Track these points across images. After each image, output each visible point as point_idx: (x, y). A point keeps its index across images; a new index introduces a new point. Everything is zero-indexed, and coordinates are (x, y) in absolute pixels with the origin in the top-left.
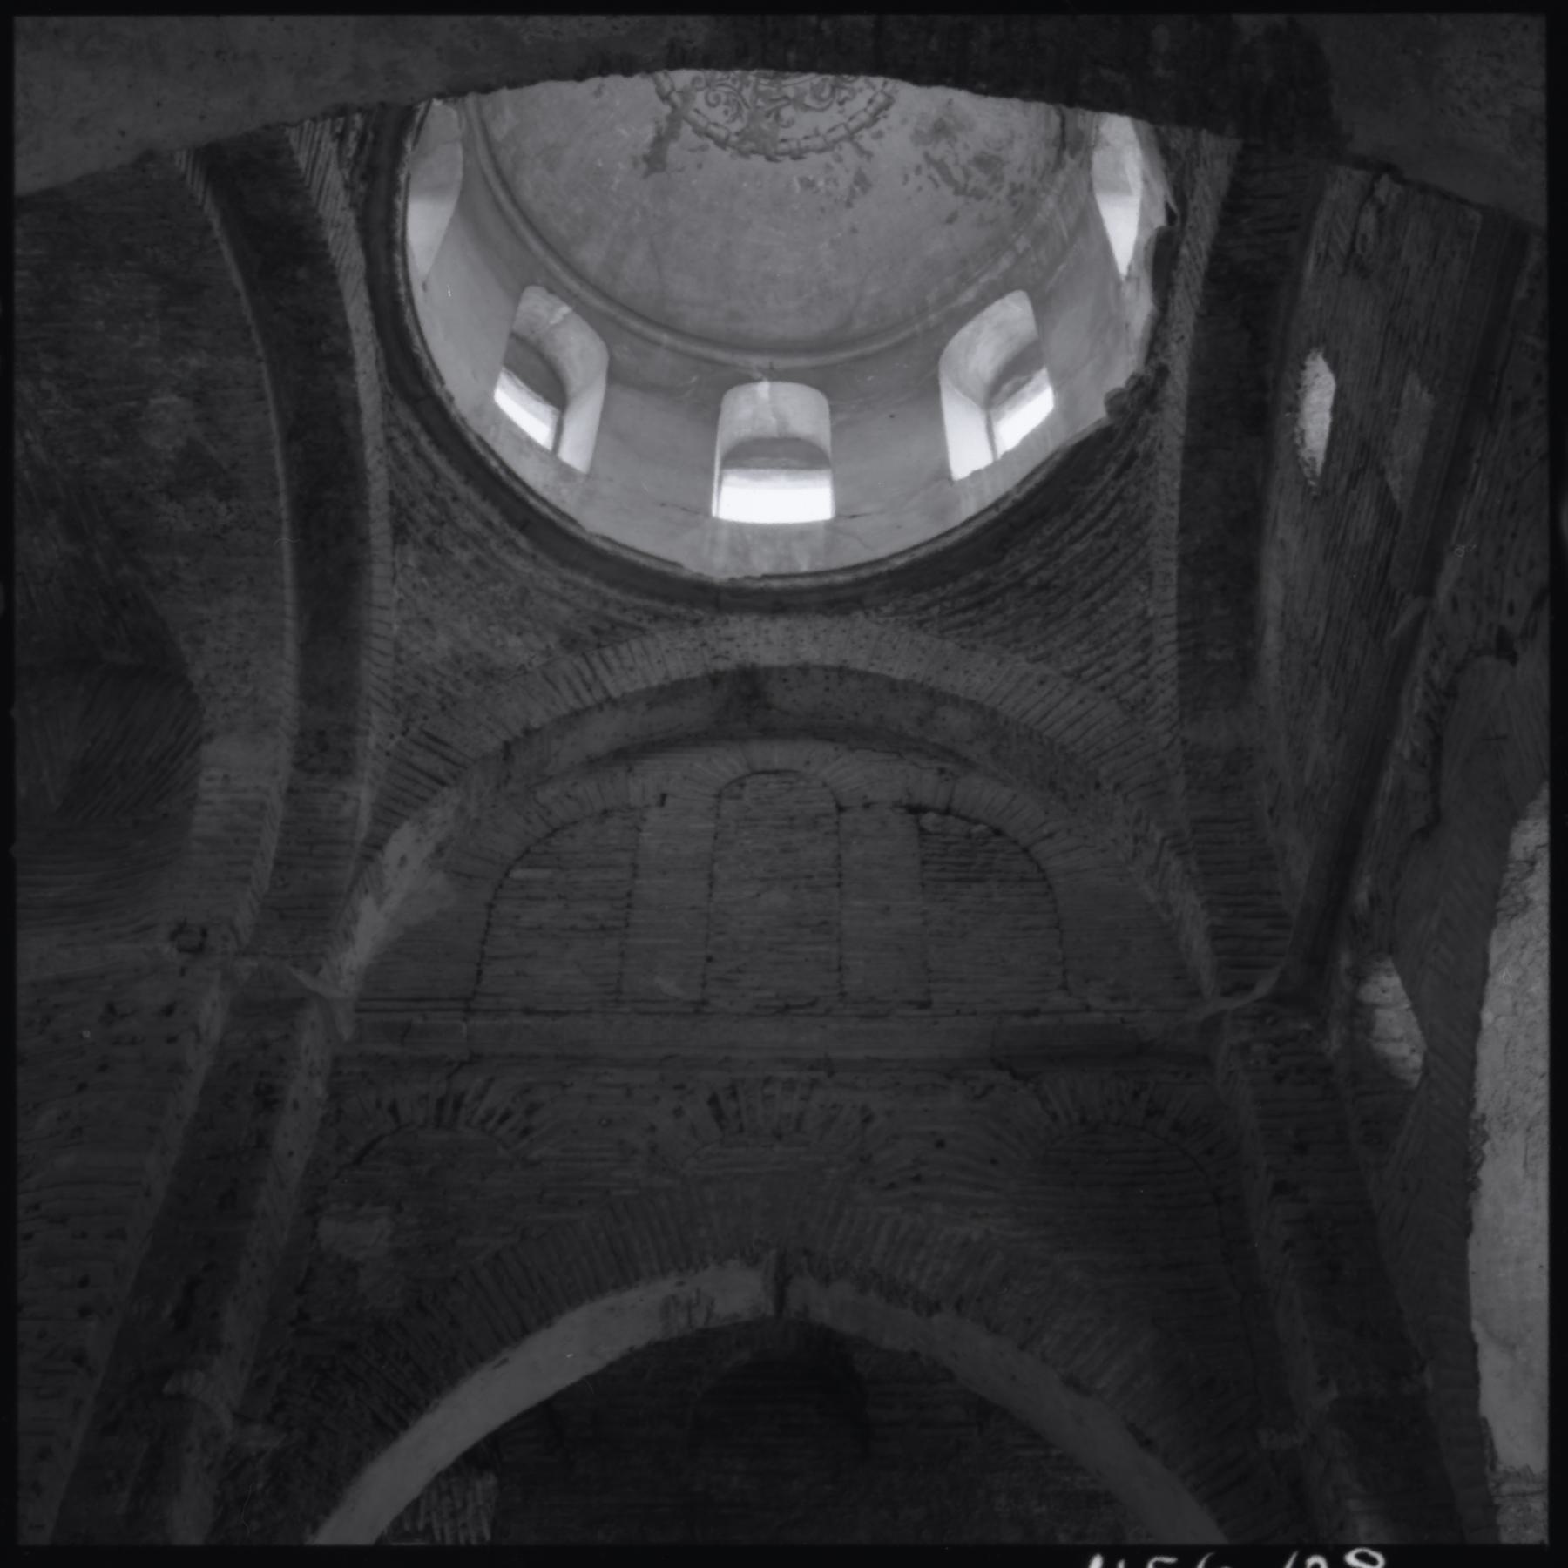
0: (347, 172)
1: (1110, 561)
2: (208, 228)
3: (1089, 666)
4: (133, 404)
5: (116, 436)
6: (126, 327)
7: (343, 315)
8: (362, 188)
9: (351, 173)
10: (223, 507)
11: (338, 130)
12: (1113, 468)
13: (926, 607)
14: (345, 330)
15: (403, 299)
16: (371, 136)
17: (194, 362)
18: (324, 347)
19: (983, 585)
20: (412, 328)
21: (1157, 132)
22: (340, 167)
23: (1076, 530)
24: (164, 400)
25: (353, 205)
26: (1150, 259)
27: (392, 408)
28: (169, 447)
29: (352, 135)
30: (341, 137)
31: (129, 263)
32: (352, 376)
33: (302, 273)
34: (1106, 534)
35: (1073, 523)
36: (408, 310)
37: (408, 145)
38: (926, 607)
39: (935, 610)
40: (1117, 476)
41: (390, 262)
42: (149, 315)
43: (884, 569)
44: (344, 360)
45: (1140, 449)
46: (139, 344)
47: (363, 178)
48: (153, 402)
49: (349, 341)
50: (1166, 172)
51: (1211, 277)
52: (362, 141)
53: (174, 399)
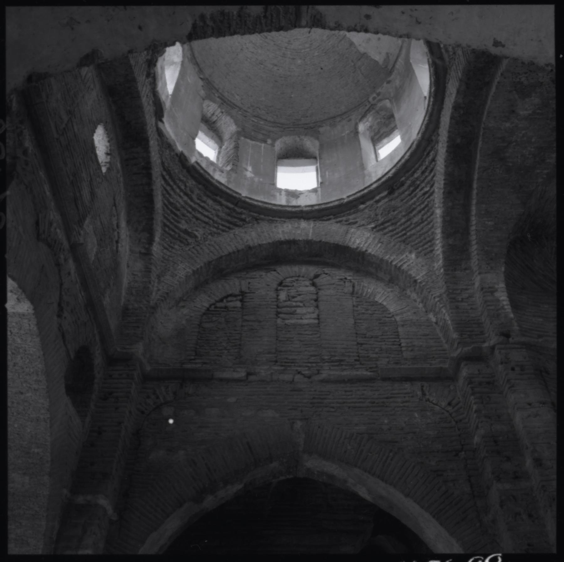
0: (436, 146)
2: (478, 179)
4: (538, 111)
5: (551, 102)
6: (525, 139)
7: (450, 123)
8: (434, 138)
9: (435, 145)
10: (523, 79)
11: (433, 163)
14: (452, 118)
15: (432, 95)
16: (425, 154)
17: (508, 125)
18: (462, 112)
20: (433, 85)
21: (173, 150)
22: (437, 150)
24: (525, 112)
25: (438, 135)
26: (163, 105)
27: (450, 62)
28: (533, 98)
29: (431, 158)
30: (434, 160)
31: (511, 164)
32: (455, 102)
33: (459, 141)
36: (433, 90)
37: (414, 146)
41: (433, 109)
42: (514, 144)
44: (456, 107)
46: (523, 132)
47: (432, 141)
48: (530, 112)
49: (452, 113)
50: (167, 139)
51: (147, 140)
52: (428, 154)
53: (521, 113)
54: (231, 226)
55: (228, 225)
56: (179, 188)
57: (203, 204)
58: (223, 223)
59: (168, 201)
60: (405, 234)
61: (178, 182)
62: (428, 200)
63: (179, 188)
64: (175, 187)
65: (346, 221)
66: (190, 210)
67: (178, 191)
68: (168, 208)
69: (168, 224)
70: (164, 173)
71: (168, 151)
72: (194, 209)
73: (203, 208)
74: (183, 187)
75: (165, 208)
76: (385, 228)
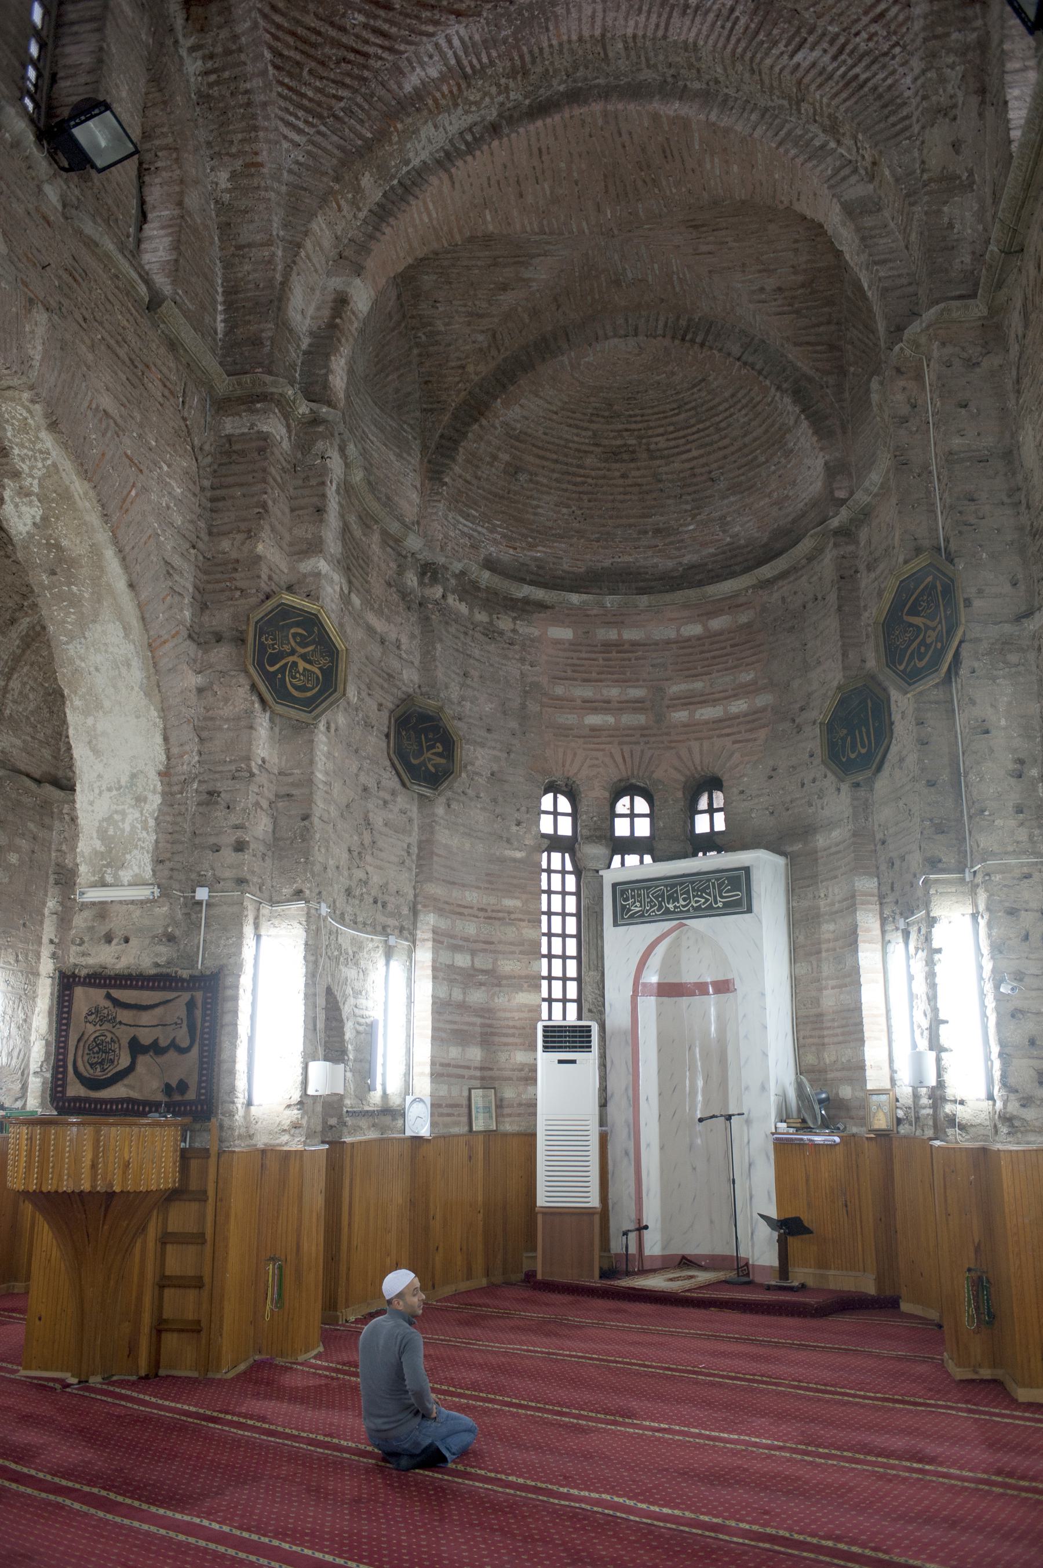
62: (380, 51)
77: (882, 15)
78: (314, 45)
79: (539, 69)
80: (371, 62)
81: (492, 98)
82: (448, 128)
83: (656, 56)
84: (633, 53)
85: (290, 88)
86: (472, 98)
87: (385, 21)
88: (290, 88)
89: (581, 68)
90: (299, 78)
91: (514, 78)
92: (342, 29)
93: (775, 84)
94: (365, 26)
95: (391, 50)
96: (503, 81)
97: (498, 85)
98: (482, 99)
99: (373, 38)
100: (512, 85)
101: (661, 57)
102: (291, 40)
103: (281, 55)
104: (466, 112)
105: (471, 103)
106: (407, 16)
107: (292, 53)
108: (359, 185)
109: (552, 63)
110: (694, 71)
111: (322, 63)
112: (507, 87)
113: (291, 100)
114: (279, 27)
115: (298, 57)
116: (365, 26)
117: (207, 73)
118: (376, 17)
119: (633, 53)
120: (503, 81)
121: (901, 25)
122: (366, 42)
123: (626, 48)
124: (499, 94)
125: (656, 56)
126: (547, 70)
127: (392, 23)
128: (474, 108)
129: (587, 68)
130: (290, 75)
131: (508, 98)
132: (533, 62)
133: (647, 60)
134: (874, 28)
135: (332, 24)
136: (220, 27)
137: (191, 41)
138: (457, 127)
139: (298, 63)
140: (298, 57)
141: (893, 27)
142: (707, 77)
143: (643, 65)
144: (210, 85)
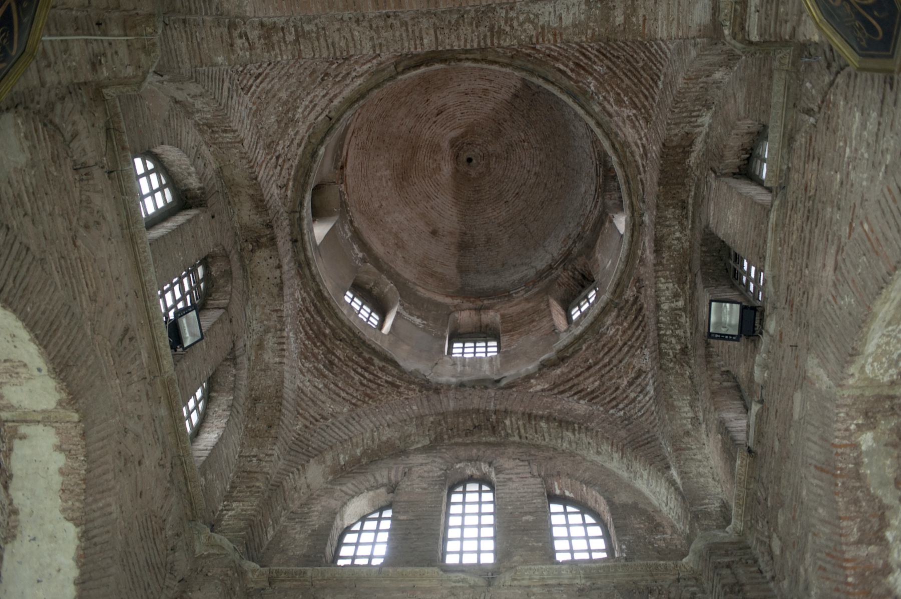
1: (352, 389)
3: (306, 396)
12: (390, 379)
13: (308, 311)
19: (325, 335)
23: (360, 370)
34: (361, 383)
35: (362, 368)
38: (308, 311)
39: (307, 315)
40: (387, 382)
43: (321, 288)
45: (402, 389)
54: (640, 318)
55: (636, 323)
56: (577, 376)
57: (606, 350)
58: (634, 327)
59: (588, 394)
60: (646, 79)
61: (571, 376)
63: (577, 376)
64: (576, 381)
65: (642, 158)
66: (608, 368)
67: (581, 378)
68: (597, 397)
69: (614, 403)
70: (556, 391)
71: (532, 381)
72: (609, 363)
73: (610, 350)
74: (580, 370)
75: (594, 401)
76: (644, 107)
77: (257, 78)
78: (630, 71)
79: (482, 29)
80: (597, 47)
81: (518, 18)
82: (552, 10)
83: (401, 35)
84: (417, 34)
85: (655, 65)
86: (531, 26)
87: (581, 60)
88: (655, 65)
89: (453, 22)
90: (646, 64)
91: (500, 27)
92: (608, 67)
93: (316, 43)
94: (595, 63)
95: (583, 47)
96: (508, 29)
97: (512, 27)
98: (524, 22)
99: (592, 57)
100: (502, 23)
101: (397, 34)
102: (643, 80)
103: (652, 79)
104: (537, 16)
105: (532, 22)
106: (567, 57)
107: (645, 75)
108: (625, 18)
109: (473, 32)
110: (374, 26)
111: (628, 61)
112: (506, 23)
113: (657, 60)
114: (647, 89)
115: (642, 72)
116: (595, 63)
117: (698, 116)
118: (586, 64)
119: (417, 34)
120: (508, 29)
121: (244, 79)
122: (596, 56)
123: (422, 39)
124: (512, 19)
125: (401, 35)
126: (477, 27)
127: (578, 58)
128: (531, 16)
129: (450, 22)
130: (651, 69)
131: (507, 13)
132: (485, 36)
133: (407, 30)
134: (261, 70)
135: (615, 73)
136: (676, 135)
137: (698, 130)
138: (546, 7)
139: (644, 70)
140: (642, 72)
141: (248, 75)
142: (364, 24)
143: (410, 23)
144: (699, 110)
